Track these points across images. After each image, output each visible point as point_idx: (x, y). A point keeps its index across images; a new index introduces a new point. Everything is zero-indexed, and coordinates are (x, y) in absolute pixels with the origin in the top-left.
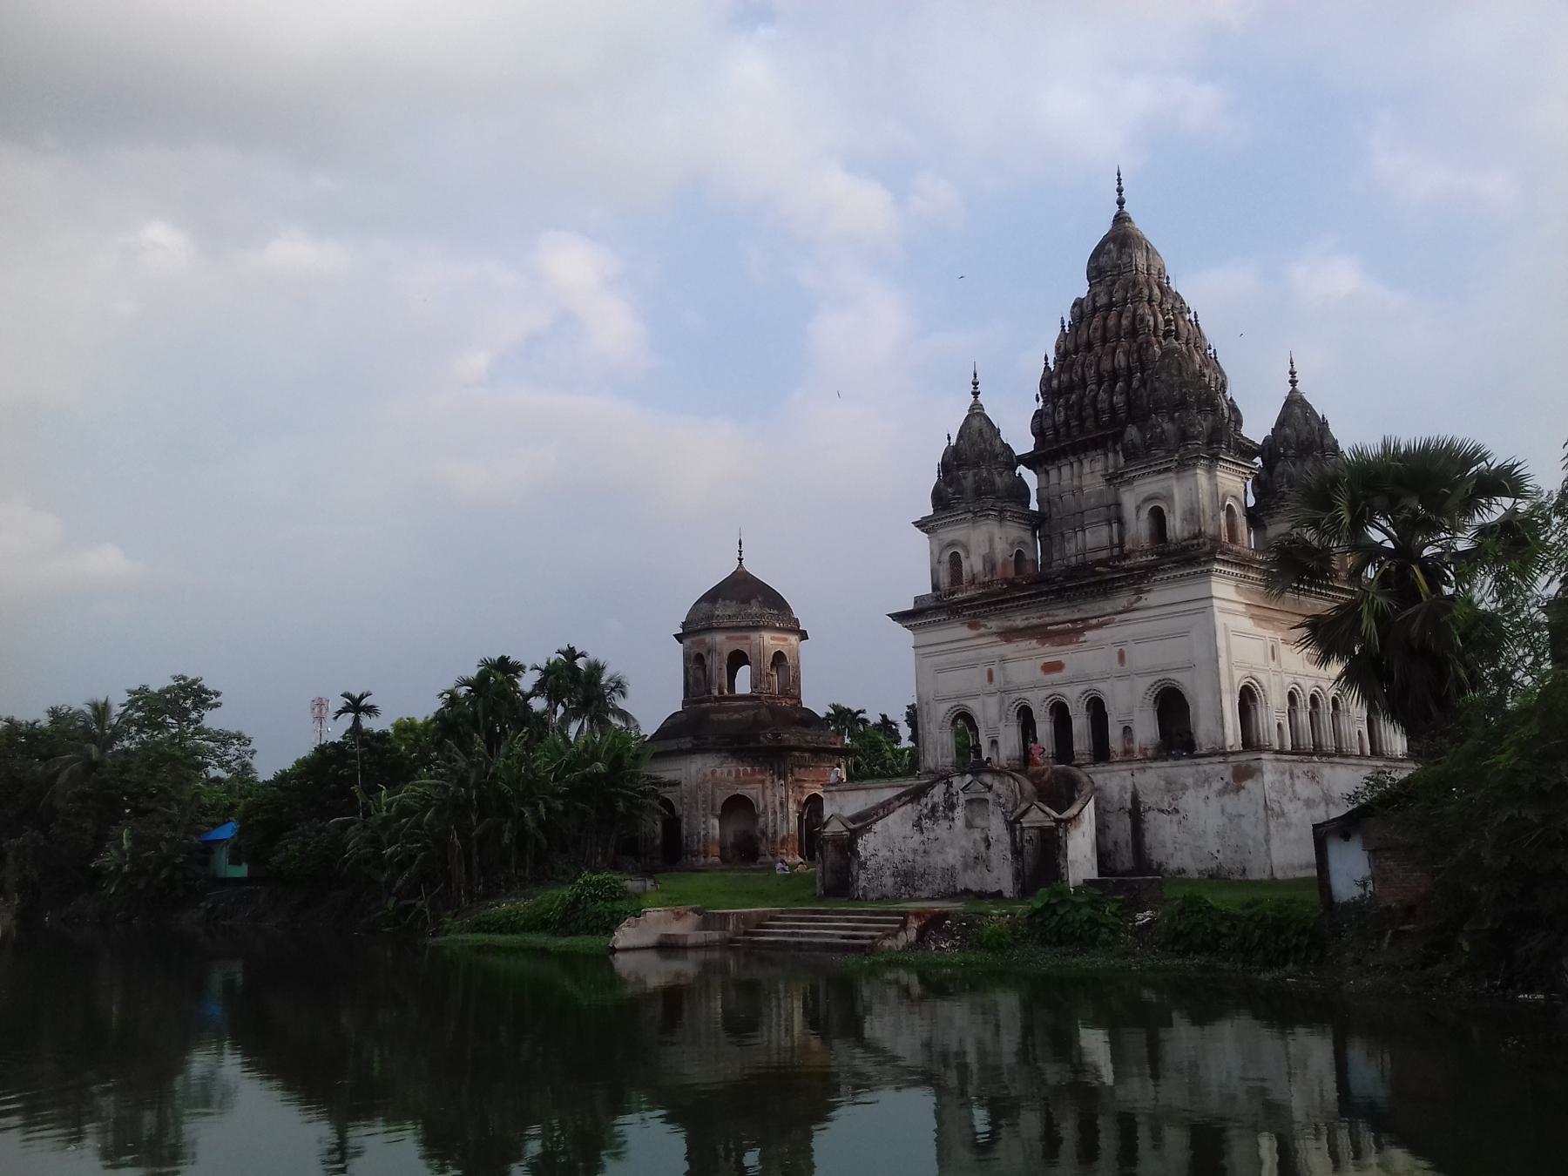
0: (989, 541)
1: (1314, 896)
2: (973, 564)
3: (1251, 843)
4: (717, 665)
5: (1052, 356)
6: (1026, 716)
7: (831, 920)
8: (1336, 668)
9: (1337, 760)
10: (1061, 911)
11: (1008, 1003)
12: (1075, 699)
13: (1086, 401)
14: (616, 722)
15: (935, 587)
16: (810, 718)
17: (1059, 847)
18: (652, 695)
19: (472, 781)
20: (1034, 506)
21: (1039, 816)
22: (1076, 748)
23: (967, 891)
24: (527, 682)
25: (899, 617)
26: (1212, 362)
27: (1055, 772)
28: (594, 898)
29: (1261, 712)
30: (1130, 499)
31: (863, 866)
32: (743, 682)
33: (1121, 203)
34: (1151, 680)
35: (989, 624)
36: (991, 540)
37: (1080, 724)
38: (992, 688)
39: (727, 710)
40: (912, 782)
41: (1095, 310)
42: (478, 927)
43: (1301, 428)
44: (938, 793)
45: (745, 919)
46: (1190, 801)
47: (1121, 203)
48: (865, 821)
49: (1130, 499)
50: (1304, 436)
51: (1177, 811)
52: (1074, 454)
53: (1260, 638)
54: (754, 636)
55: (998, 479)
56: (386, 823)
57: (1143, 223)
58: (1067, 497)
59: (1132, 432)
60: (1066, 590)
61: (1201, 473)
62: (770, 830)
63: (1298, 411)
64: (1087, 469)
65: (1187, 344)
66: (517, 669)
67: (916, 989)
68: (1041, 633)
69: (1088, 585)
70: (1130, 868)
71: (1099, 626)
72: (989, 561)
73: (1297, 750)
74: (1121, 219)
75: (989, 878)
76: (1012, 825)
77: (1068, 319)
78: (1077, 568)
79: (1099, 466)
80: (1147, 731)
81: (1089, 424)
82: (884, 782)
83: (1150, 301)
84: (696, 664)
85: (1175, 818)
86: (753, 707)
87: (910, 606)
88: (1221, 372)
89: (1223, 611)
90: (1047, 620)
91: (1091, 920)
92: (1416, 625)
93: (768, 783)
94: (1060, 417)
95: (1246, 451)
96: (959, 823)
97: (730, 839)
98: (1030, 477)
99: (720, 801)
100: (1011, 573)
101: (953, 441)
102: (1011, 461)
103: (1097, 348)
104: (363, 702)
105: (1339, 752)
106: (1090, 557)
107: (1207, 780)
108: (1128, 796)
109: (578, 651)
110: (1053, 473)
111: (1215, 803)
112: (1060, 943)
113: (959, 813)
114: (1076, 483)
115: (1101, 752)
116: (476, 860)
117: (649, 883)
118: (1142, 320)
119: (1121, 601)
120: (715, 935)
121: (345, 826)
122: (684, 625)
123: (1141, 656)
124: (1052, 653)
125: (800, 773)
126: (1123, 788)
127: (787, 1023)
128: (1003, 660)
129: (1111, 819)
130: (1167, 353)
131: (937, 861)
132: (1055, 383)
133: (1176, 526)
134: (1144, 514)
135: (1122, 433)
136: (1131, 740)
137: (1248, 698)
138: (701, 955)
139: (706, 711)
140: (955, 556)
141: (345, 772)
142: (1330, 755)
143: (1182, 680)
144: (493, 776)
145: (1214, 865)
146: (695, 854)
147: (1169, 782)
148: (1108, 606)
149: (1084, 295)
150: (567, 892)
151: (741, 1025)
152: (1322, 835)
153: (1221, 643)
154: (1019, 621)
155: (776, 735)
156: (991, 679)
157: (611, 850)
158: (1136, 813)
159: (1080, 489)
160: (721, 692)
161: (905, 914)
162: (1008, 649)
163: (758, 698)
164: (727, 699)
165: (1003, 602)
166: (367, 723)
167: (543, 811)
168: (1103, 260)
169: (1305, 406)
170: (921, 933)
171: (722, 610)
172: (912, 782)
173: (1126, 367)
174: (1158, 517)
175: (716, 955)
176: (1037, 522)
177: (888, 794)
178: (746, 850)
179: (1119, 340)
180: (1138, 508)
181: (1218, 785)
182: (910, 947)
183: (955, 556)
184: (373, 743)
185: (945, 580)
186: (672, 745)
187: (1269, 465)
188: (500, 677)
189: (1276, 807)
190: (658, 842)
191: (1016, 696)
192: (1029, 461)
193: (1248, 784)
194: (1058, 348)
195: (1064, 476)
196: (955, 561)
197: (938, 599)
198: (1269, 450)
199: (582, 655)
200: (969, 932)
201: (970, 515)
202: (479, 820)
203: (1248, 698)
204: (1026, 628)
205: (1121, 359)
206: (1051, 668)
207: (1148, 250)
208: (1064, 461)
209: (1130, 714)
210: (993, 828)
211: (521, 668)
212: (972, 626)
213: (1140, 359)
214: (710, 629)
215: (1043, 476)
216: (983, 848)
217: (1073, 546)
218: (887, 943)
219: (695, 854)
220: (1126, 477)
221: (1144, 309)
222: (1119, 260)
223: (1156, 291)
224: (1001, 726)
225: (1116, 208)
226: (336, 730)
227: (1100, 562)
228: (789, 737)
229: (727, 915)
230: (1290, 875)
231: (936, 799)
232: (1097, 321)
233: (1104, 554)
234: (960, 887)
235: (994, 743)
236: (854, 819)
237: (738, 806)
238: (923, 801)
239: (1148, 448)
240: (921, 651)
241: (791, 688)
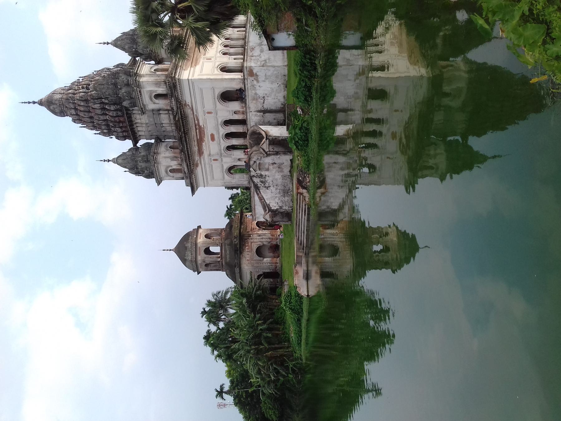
0: (166, 158)
1: (293, 52)
2: (174, 164)
3: (275, 72)
4: (209, 259)
5: (95, 132)
7: (299, 219)
8: (214, 37)
9: (247, 40)
10: (297, 139)
11: (327, 159)
13: (113, 120)
14: (228, 296)
15: (183, 179)
16: (230, 225)
17: (276, 139)
18: (219, 282)
19: (249, 348)
20: (153, 141)
21: (265, 145)
22: (242, 131)
23: (290, 171)
24: (213, 328)
25: (193, 192)
26: (99, 73)
27: (250, 139)
28: (290, 303)
29: (229, 65)
30: (151, 106)
31: (281, 207)
32: (215, 249)
33: (34, 103)
34: (218, 103)
35: (197, 159)
36: (165, 157)
37: (233, 129)
38: (220, 160)
39: (226, 255)
40: (253, 189)
41: (77, 115)
42: (299, 344)
43: (125, 42)
44: (256, 180)
45: (298, 249)
46: (260, 92)
47: (34, 103)
48: (266, 206)
49: (151, 106)
50: (129, 41)
51: (264, 97)
52: (133, 125)
53: (203, 63)
54: (199, 245)
55: (142, 154)
56: (263, 379)
57: (43, 95)
59: (126, 104)
60: (184, 131)
61: (142, 80)
62: (269, 240)
63: (119, 43)
64: (139, 121)
65: (92, 81)
66: (208, 331)
67: (322, 190)
68: (200, 141)
69: (183, 123)
70: (284, 115)
71: (198, 120)
73: (243, 54)
74: (41, 103)
75: (285, 164)
76: (268, 155)
77: (80, 125)
78: (177, 127)
79: (138, 117)
80: (235, 106)
81: (122, 119)
82: (252, 199)
83: (74, 94)
84: (208, 267)
85: (266, 98)
86: (225, 246)
87: (189, 188)
88: (103, 69)
89: (193, 75)
90: (195, 139)
91: (300, 129)
92: (200, 8)
93: (252, 241)
94: (119, 130)
95: (134, 62)
96: (267, 173)
97: (271, 254)
98: (141, 142)
99: (257, 258)
100: (178, 151)
101: (127, 170)
102: (135, 148)
103: (93, 115)
104: (219, 390)
105: (244, 39)
106: (172, 122)
107: (253, 86)
108: (259, 114)
109: (202, 310)
110: (140, 133)
111: (261, 84)
112: (308, 140)
113: (263, 173)
114: (144, 125)
115: (243, 122)
116: (276, 346)
117: (285, 283)
118: (82, 97)
119: (188, 111)
120: (304, 260)
121: (264, 394)
122: (194, 271)
123: (209, 106)
124: (207, 138)
125: (249, 229)
126: (256, 115)
127: (334, 236)
128: (210, 155)
129: (266, 120)
130: (95, 89)
131: (280, 181)
132: (105, 131)
133: (162, 90)
134: (157, 101)
135: (125, 107)
136: (239, 111)
137: (224, 69)
138: (310, 265)
139: (226, 263)
140: (171, 171)
141: (244, 395)
142: (245, 43)
143: (218, 92)
144: (247, 340)
145: (282, 86)
146: (276, 267)
147: (254, 99)
148: (191, 117)
149: (71, 119)
150: (288, 312)
151: (335, 251)
152: (273, 48)
153: (205, 77)
154: (196, 149)
155: (235, 238)
156: (216, 160)
157: (274, 297)
158: (265, 111)
159: (147, 124)
160: (219, 257)
161: (298, 193)
162: (206, 153)
163: (222, 244)
164: (221, 255)
165: (188, 154)
166: (226, 388)
167: (260, 322)
168: (57, 110)
169: (117, 40)
170: (304, 188)
171: (189, 257)
172: (253, 189)
173: (101, 104)
174: (158, 96)
175: (310, 260)
176: (159, 140)
177: (256, 198)
178: (275, 248)
179: (89, 106)
180: (154, 103)
181: (255, 82)
182: (308, 192)
183: (171, 171)
184: (234, 385)
185: (180, 175)
186: (238, 275)
187: (140, 55)
188: (211, 339)
189: (263, 63)
190: (272, 280)
191: (223, 152)
192: (135, 142)
193: (255, 71)
194: (92, 129)
195: (141, 129)
196: (173, 171)
197: (187, 178)
198: (134, 54)
199: (204, 309)
200: (303, 172)
201: (156, 165)
202: (262, 345)
203: (224, 69)
204: (198, 146)
206: (213, 138)
207: (54, 93)
208: (136, 129)
209: (230, 111)
210: (269, 161)
211: (208, 331)
212: (197, 166)
213: (97, 99)
214: (196, 261)
215: (141, 137)
216: (275, 165)
217: (168, 128)
218: (307, 200)
219: (276, 267)
220: (142, 107)
221: (77, 96)
222: (57, 105)
223: (70, 91)
224: (233, 157)
225: (36, 104)
226: (229, 399)
227: (175, 118)
228: (236, 233)
229: (297, 255)
230: (286, 59)
231: (259, 181)
232: (82, 114)
233: (172, 117)
234: (289, 174)
235: (239, 160)
236: (265, 210)
237: (259, 252)
238: (259, 185)
239: (132, 98)
240: (206, 184)
241: (218, 232)
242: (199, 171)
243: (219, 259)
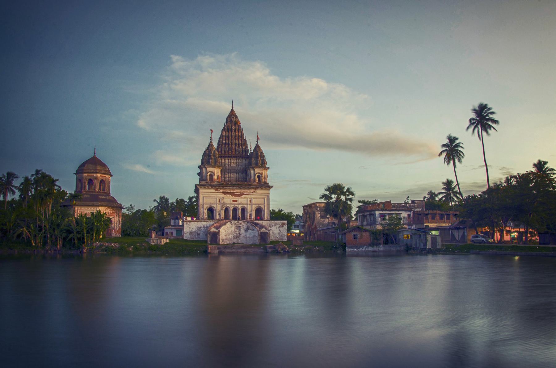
2: (215, 177)
6: (227, 210)
12: (240, 207)
33: (232, 107)
46: (273, 228)
47: (232, 107)
58: (227, 166)
64: (232, 161)
68: (233, 194)
72: (218, 176)
74: (232, 111)
81: (234, 153)
84: (79, 181)
111: (278, 229)
119: (252, 191)
128: (223, 198)
133: (262, 180)
148: (249, 191)
154: (228, 191)
205: (240, 141)
209: (252, 211)
242: (213, 190)
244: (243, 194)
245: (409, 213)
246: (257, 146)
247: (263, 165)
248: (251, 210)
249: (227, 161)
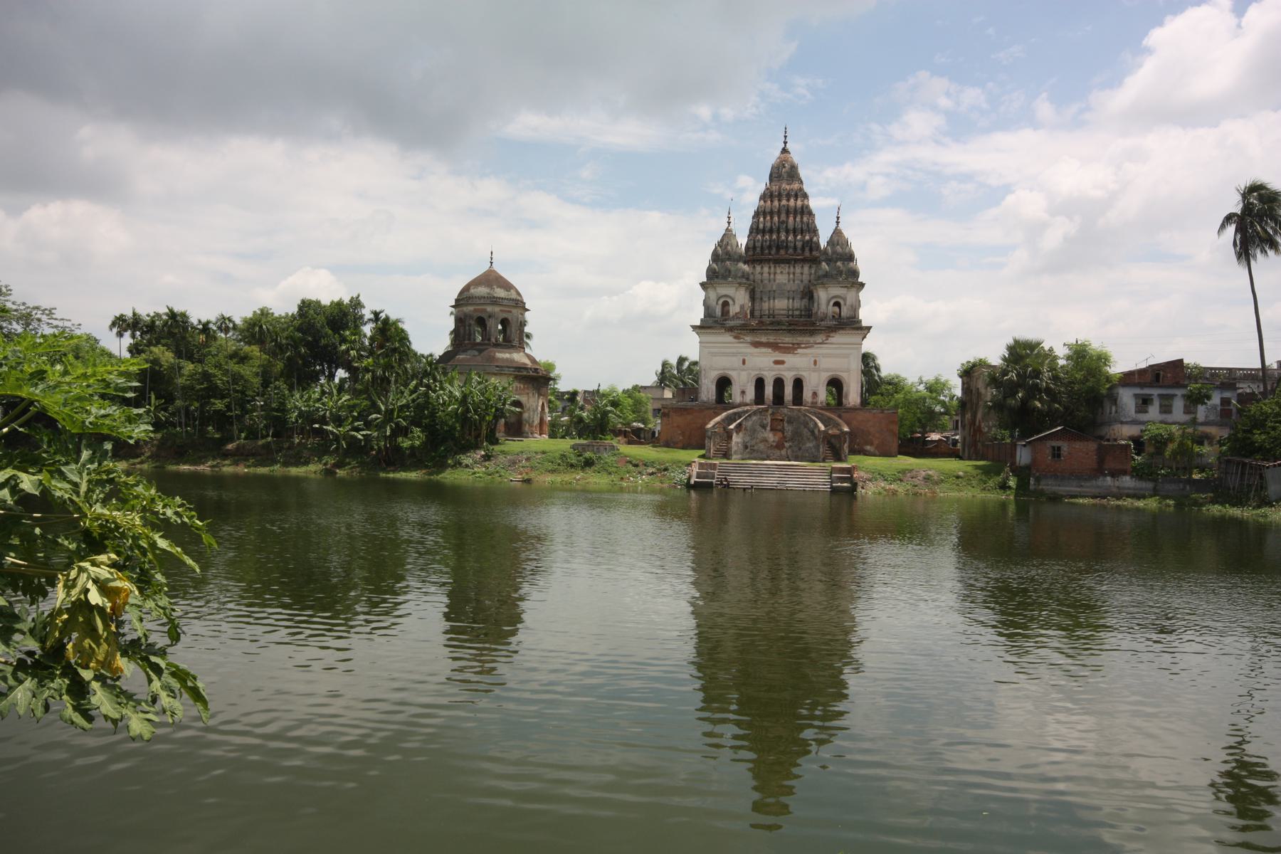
2: (734, 309)
6: (760, 383)
25: (694, 328)
68: (775, 346)
72: (742, 307)
74: (785, 151)
87: (698, 323)
119: (819, 339)
124: (780, 357)
132: (761, 226)
143: (844, 376)
148: (811, 340)
154: (764, 339)
180: (828, 302)
196: (725, 304)
206: (777, 362)
235: (743, 392)
242: (728, 338)
243: (493, 340)
244: (799, 345)
245: (1227, 394)
246: (837, 232)
247: (852, 279)
248: (815, 386)
249: (766, 269)
